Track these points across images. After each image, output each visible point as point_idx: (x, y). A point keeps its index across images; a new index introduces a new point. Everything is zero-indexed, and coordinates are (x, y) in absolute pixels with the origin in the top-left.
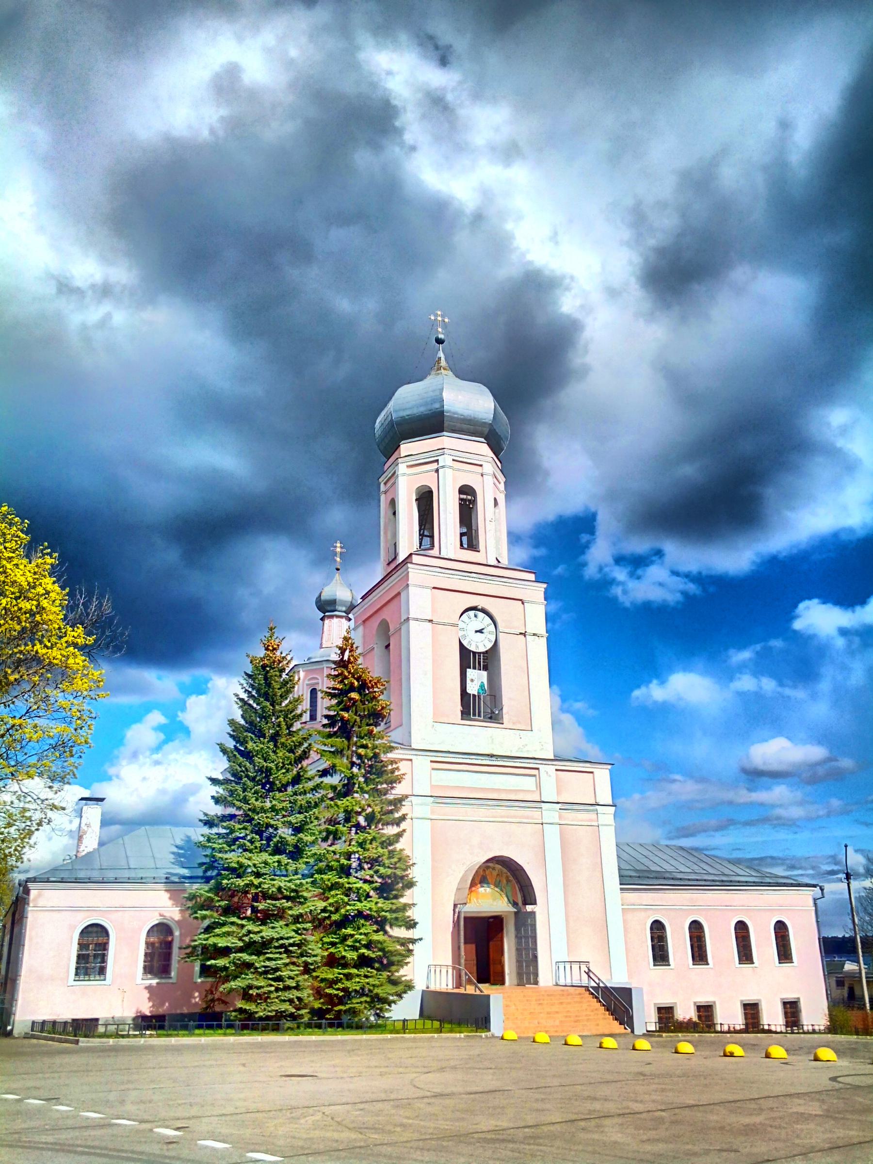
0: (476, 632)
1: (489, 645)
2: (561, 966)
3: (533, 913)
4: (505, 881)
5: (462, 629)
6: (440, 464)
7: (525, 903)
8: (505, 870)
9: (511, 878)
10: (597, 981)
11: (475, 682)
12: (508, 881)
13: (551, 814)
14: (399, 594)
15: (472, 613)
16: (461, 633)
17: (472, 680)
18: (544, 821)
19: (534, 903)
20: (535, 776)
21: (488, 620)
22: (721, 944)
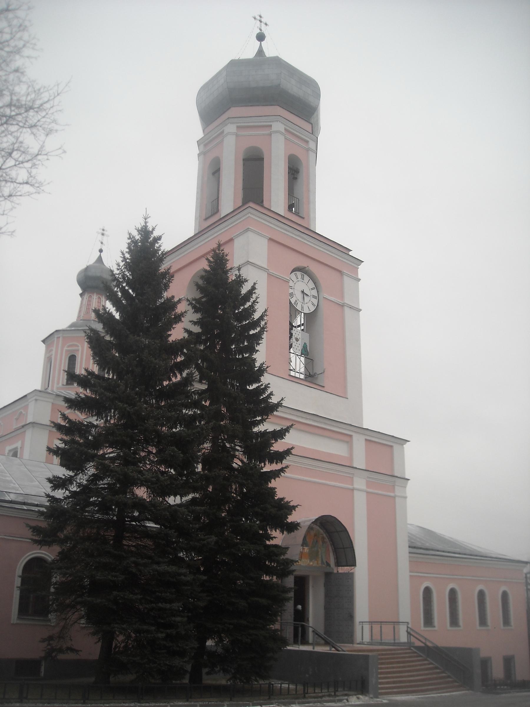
0: (303, 292)
1: (312, 309)
2: (367, 627)
3: (350, 577)
4: (321, 543)
5: (291, 287)
6: (274, 128)
7: (338, 564)
8: (321, 531)
9: (327, 540)
10: (424, 641)
11: (299, 342)
12: (324, 542)
13: (360, 483)
14: (231, 240)
15: (299, 274)
16: (291, 291)
17: (297, 340)
18: (356, 486)
19: (354, 564)
20: (347, 442)
21: (311, 285)
22: (467, 609)
